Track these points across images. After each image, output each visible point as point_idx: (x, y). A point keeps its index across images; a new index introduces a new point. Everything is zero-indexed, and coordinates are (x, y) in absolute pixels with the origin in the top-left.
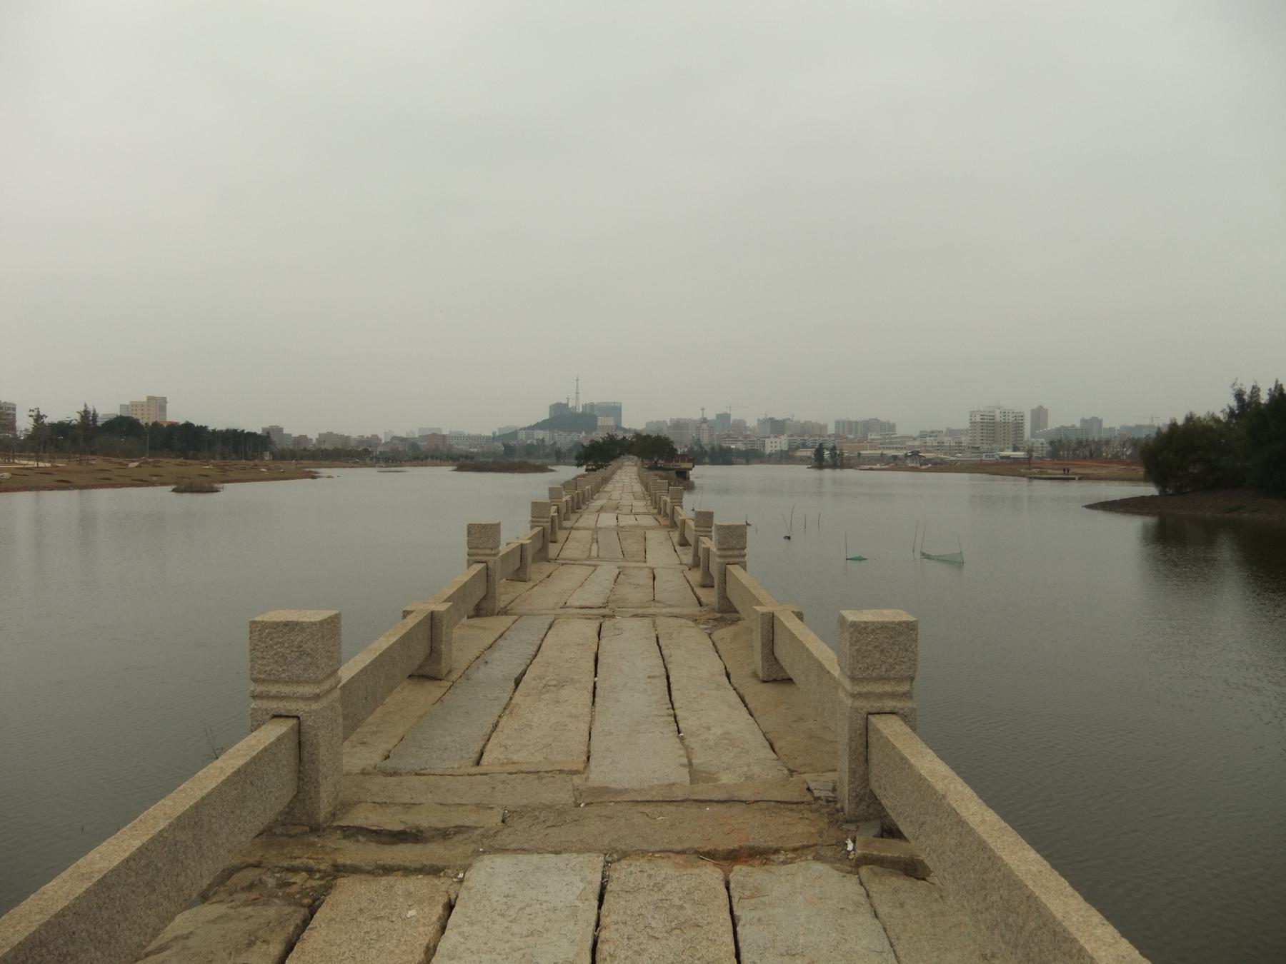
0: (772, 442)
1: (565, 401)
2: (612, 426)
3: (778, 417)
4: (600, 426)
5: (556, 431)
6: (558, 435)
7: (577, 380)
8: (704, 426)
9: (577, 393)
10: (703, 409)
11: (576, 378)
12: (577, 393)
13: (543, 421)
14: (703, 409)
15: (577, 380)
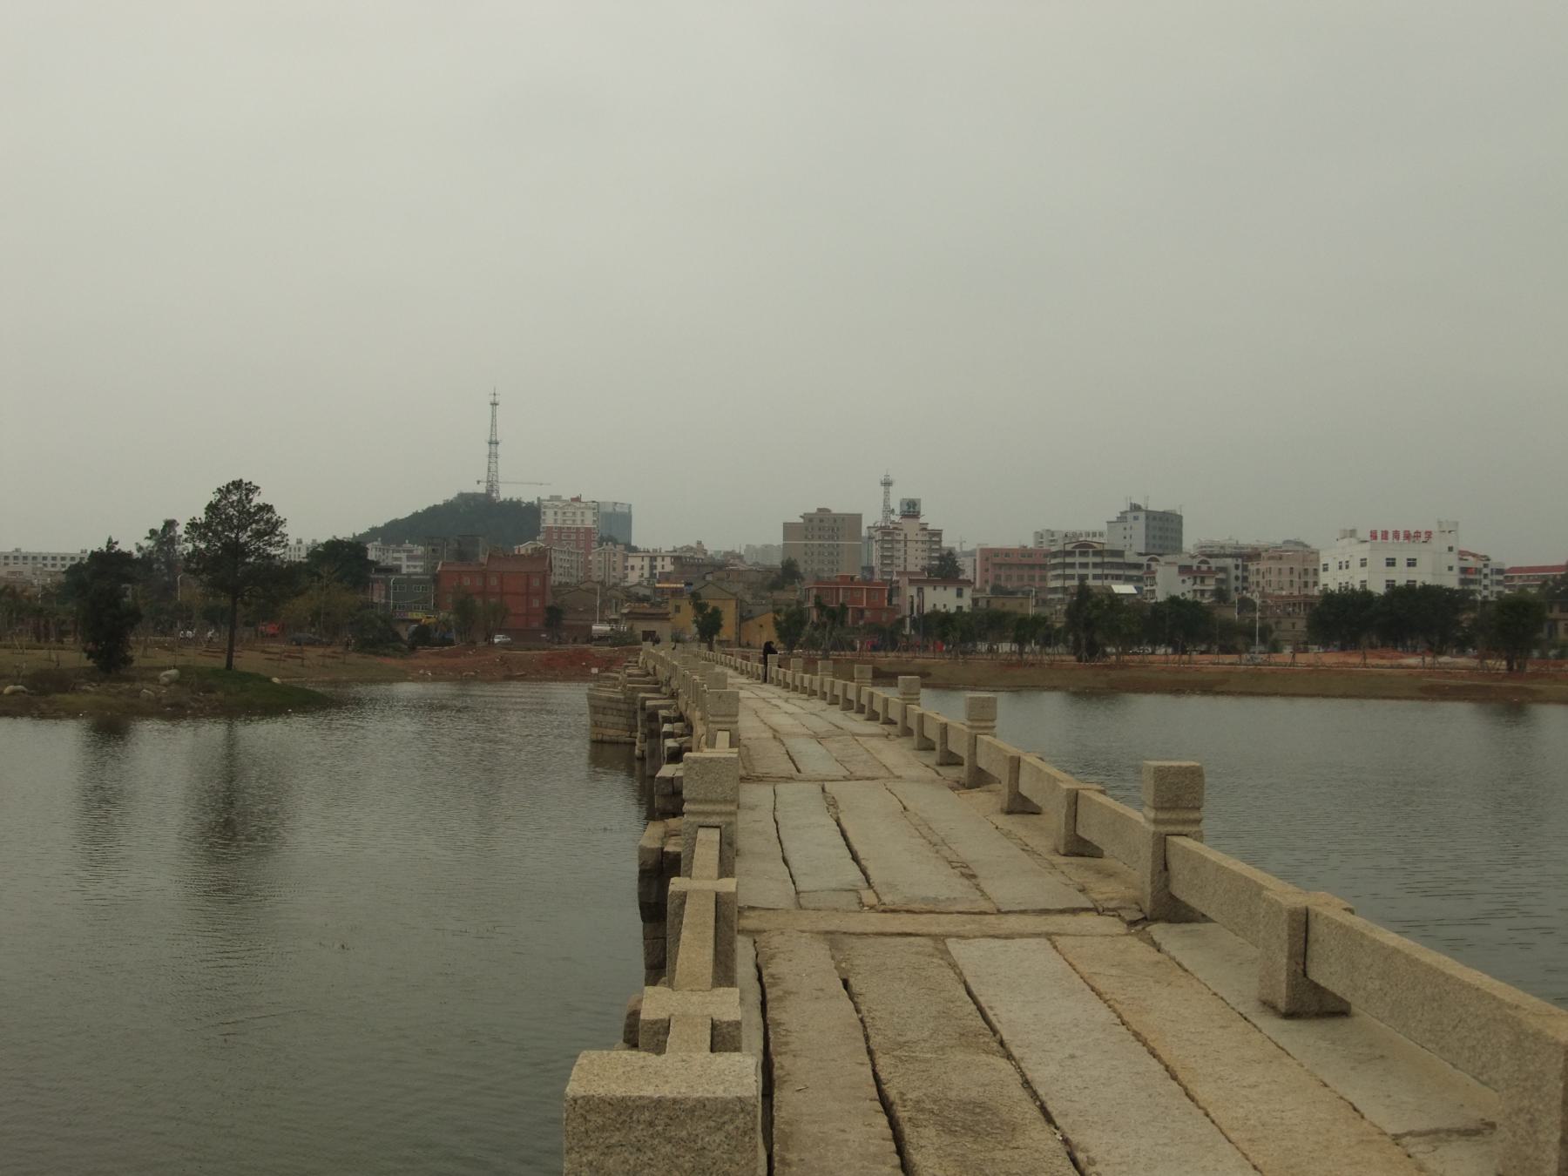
0: (1391, 563)
1: (481, 489)
2: (588, 530)
3: (1156, 506)
4: (550, 528)
5: (407, 545)
6: (409, 558)
7: (494, 404)
8: (910, 527)
9: (493, 443)
10: (887, 484)
11: (492, 398)
12: (493, 443)
13: (386, 525)
14: (887, 484)
15: (494, 404)
